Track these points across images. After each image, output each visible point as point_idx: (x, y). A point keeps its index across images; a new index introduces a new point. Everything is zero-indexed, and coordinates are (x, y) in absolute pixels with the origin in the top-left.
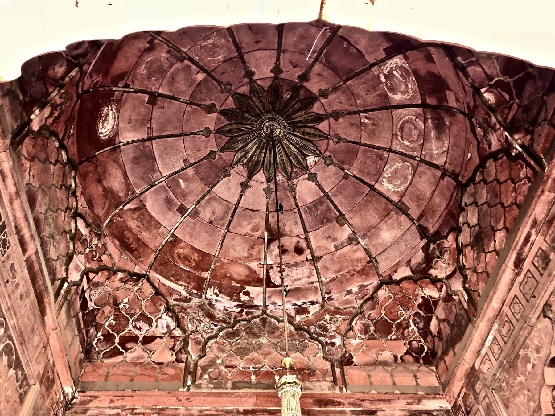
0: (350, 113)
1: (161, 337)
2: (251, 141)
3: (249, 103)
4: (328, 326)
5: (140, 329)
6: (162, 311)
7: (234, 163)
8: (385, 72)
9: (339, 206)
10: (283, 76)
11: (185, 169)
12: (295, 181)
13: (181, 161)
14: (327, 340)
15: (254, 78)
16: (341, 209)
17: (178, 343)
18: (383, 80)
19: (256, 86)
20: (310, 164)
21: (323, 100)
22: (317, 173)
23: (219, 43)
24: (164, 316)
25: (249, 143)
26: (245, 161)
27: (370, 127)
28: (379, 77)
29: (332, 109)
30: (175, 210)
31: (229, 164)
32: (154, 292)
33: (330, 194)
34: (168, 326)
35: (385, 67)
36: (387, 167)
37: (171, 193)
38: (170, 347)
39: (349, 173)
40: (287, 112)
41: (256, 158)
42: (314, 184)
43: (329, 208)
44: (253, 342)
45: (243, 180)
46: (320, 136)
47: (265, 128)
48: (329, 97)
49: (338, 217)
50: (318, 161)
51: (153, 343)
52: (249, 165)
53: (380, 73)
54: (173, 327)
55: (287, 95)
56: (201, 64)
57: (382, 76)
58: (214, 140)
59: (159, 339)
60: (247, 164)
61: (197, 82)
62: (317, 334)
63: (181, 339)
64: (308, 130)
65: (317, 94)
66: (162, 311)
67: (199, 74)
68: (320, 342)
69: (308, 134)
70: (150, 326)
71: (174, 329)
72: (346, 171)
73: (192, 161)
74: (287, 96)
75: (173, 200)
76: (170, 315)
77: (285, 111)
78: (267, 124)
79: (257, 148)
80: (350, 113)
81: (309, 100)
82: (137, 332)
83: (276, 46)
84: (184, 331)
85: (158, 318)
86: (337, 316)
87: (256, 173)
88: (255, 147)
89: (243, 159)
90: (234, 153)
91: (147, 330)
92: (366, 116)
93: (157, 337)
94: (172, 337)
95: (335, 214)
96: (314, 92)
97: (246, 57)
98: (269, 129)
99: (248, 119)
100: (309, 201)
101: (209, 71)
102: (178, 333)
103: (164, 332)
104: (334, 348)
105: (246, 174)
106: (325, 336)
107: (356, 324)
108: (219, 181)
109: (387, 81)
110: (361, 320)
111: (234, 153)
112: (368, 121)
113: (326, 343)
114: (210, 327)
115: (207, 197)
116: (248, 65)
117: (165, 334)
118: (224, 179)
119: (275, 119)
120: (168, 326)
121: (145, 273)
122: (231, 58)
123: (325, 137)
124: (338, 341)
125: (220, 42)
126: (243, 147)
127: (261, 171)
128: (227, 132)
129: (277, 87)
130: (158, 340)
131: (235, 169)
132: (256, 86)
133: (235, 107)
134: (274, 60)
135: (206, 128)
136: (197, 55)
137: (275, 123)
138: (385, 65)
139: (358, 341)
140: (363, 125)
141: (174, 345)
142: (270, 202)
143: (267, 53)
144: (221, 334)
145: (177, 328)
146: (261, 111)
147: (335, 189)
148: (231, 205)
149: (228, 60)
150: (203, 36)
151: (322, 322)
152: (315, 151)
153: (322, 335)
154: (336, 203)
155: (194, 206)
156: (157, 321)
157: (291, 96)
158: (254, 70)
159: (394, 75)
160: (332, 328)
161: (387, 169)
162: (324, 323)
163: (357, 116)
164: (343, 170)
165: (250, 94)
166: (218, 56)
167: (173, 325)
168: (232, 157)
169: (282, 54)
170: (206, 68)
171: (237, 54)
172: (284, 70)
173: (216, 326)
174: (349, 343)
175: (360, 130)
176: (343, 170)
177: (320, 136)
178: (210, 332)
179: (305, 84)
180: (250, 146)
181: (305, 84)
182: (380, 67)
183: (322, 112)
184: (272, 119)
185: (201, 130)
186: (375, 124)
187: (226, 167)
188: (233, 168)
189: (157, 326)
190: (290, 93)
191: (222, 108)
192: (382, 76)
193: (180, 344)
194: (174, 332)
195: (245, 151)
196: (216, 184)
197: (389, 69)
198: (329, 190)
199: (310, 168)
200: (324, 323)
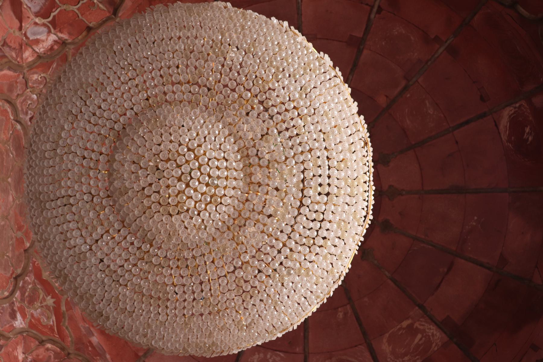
1: (20, 28)
4: (37, 304)
6: (60, 35)
14: (17, 305)
17: (14, 55)
24: (53, 37)
32: (91, 25)
34: (37, 41)
36: (282, 354)
38: (8, 41)
44: (9, 180)
51: (12, 14)
54: (37, 50)
59: (19, 25)
62: (23, 287)
63: (18, 59)
68: (12, 293)
70: (37, 15)
71: (34, 50)
76: (56, 47)
84: (32, 67)
85: (49, 27)
86: (54, 318)
91: (30, 8)
93: (21, 22)
94: (21, 46)
102: (28, 55)
103: (29, 34)
104: (8, 317)
106: (22, 300)
107: (48, 349)
110: (55, 358)
113: (13, 303)
114: (30, 109)
117: (25, 35)
120: (37, 41)
121: (120, 15)
124: (19, 323)
130: (16, 22)
139: (21, 357)
141: (10, 47)
144: (19, 127)
145: (36, 55)
151: (42, 295)
153: (23, 294)
156: (44, 25)
160: (36, 312)
161: (279, 355)
162: (41, 297)
167: (40, 49)
173: (31, 119)
174: (17, 344)
178: (22, 110)
189: (36, 24)
193: (12, 57)
194: (30, 50)
200: (41, 297)
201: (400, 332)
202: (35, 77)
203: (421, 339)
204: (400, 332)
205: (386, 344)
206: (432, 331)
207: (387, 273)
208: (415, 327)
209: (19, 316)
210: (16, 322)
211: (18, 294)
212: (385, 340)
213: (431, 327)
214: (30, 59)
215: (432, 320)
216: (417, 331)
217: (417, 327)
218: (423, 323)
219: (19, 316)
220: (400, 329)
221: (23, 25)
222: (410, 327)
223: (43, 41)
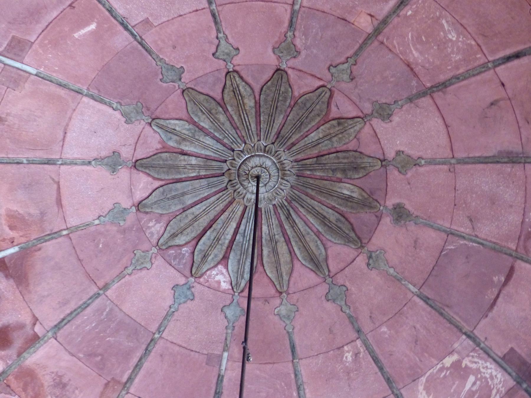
0: (352, 320)
2: (218, 140)
3: (313, 120)
7: (161, 122)
8: (466, 362)
9: (142, 372)
10: (394, 174)
11: (126, 28)
12: (159, 261)
13: (145, 16)
15: (376, 123)
16: (137, 380)
18: (448, 361)
19: (357, 128)
20: (210, 276)
21: (361, 261)
22: (197, 300)
23: (449, 50)
25: (214, 138)
26: (171, 144)
27: (339, 367)
28: (451, 353)
29: (347, 284)
30: (14, 33)
31: (158, 113)
33: (161, 343)
35: (476, 360)
37: (55, 14)
39: (224, 362)
40: (307, 195)
41: (184, 163)
42: (169, 302)
43: (127, 355)
45: (126, 153)
46: (280, 276)
47: (256, 161)
48: (374, 274)
49: (119, 382)
50: (224, 292)
52: (164, 155)
53: (458, 353)
55: (348, 189)
56: (395, 20)
57: (455, 357)
58: (208, 71)
60: (166, 149)
61: (351, 19)
64: (282, 248)
65: (371, 247)
67: (369, 18)
69: (275, 251)
72: (226, 355)
73: (149, 40)
74: (346, 189)
75: (38, 22)
77: (309, 191)
78: (268, 163)
79: (207, 158)
80: (352, 320)
81: (352, 235)
83: (460, 155)
87: (149, 175)
88: (208, 153)
89: (175, 137)
90: (184, 115)
92: (359, 353)
95: (123, 372)
96: (374, 240)
97: (426, 101)
98: (259, 169)
99: (271, 122)
100: (126, 307)
101: (380, 38)
105: (139, 155)
108: (110, 105)
109: (447, 369)
111: (184, 115)
112: (350, 359)
115: (62, 92)
116: (404, 108)
118: (117, 114)
119: (284, 175)
122: (415, 75)
123: (282, 286)
125: (453, 52)
126: (202, 129)
127: (157, 184)
128: (235, 92)
129: (364, 168)
131: (148, 128)
132: (357, 128)
133: (296, 94)
134: (429, 154)
135: (238, 49)
136: (416, 12)
137: (274, 179)
138: (479, 357)
140: (337, 352)
142: (93, 229)
143: (443, 140)
146: (293, 144)
147: (177, 348)
148: (57, 148)
149: (412, 69)
150: (464, 22)
152: (242, 277)
154: (146, 365)
155: (33, 71)
157: (348, 199)
158: (396, 119)
159: (465, 378)
163: (355, 335)
164: (226, 348)
165: (334, 119)
166: (416, 49)
168: (174, 115)
169: (446, 167)
170: (386, 30)
171: (429, 85)
172: (409, 174)
175: (324, 349)
176: (226, 348)
177: (280, 276)
179: (387, 221)
180: (208, 141)
181: (387, 221)
182: (474, 350)
183: (333, 266)
184: (281, 169)
185: (231, 40)
186: (348, 373)
187: (148, 110)
188: (150, 124)
190: (354, 195)
191: (290, 71)
192: (455, 357)
195: (193, 137)
196: (102, 102)
197: (474, 366)
198: (169, 338)
199: (202, 280)
201: (443, 374)
203: (474, 383)
204: (443, 374)
205: (424, 393)
206: (489, 371)
207: (411, 287)
208: (463, 365)
212: (421, 388)
213: (488, 364)
215: (488, 353)
216: (467, 372)
217: (466, 366)
218: (476, 360)
220: (441, 370)
222: (456, 365)
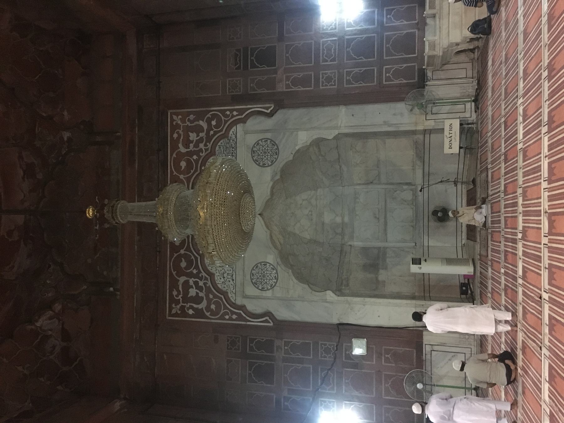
1: (63, 324)
5: (54, 347)
6: (33, 327)
24: (38, 324)
34: (50, 318)
54: (51, 312)
66: (33, 327)
76: (37, 318)
82: (58, 349)
102: (58, 307)
117: (59, 320)
120: (50, 318)
173: (50, 266)
202: (50, 295)
209: (66, 139)
210: (68, 135)
211: (64, 152)
214: (57, 305)
219: (66, 139)
221: (61, 326)
223: (46, 320)
